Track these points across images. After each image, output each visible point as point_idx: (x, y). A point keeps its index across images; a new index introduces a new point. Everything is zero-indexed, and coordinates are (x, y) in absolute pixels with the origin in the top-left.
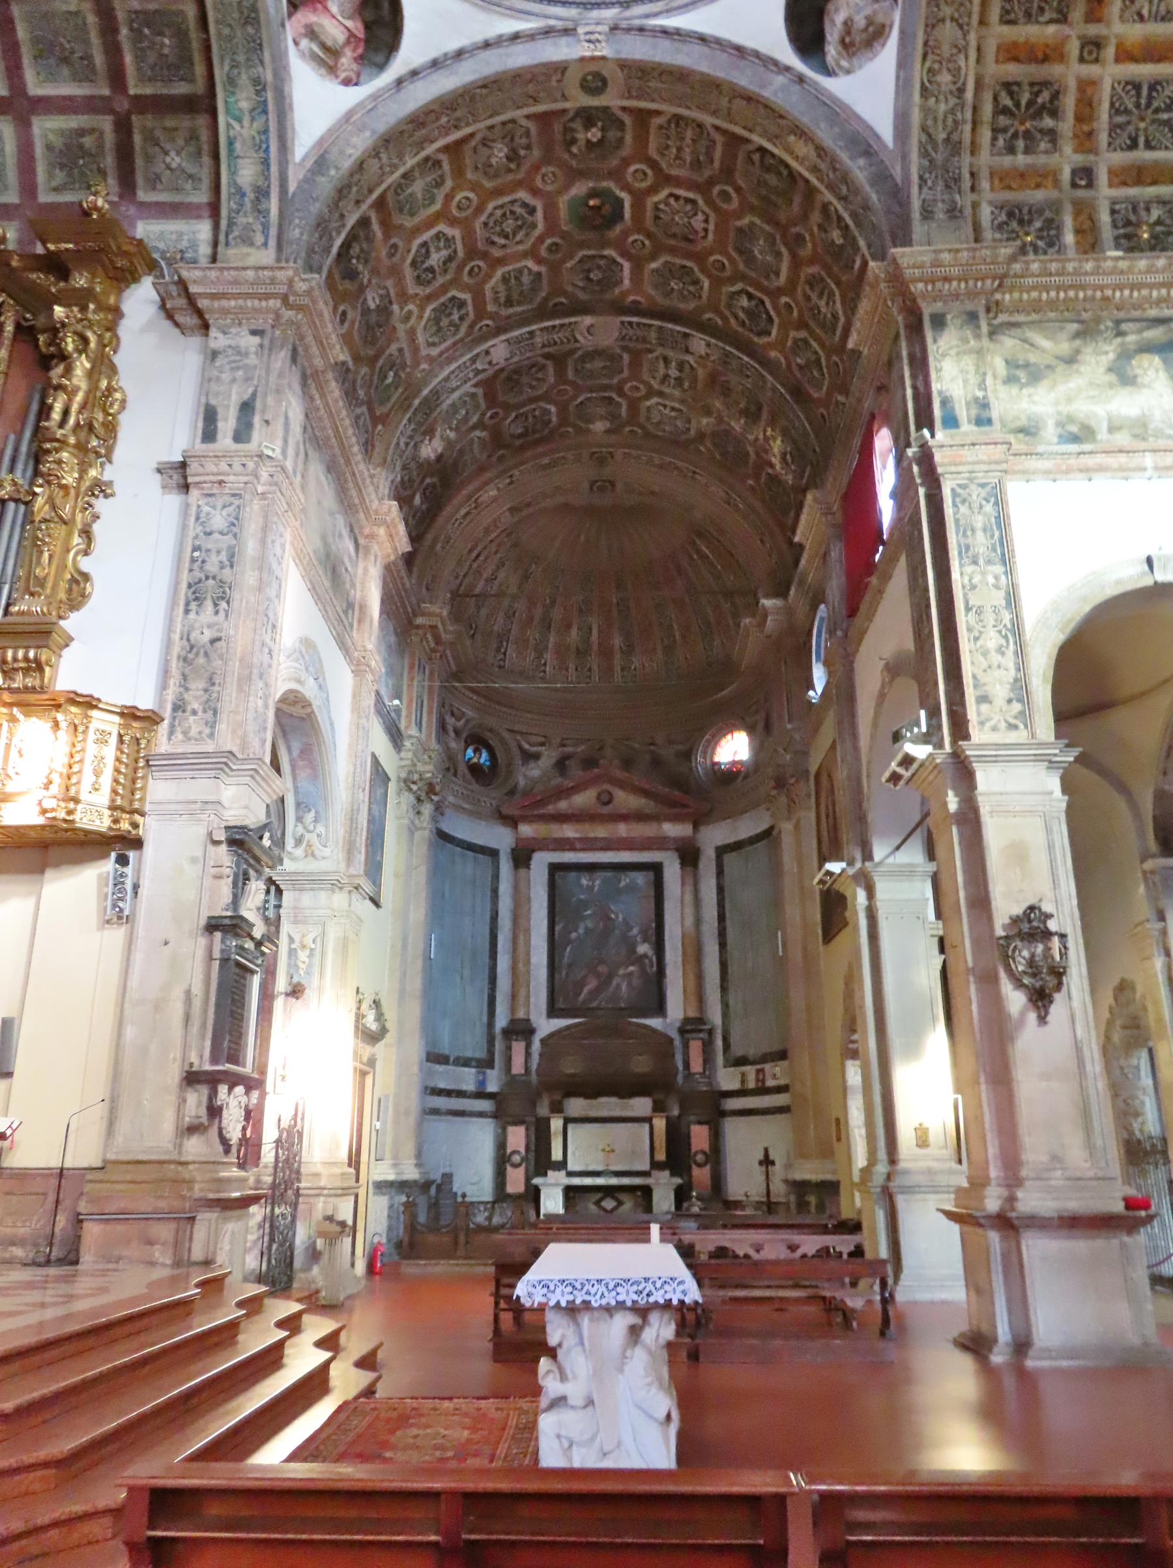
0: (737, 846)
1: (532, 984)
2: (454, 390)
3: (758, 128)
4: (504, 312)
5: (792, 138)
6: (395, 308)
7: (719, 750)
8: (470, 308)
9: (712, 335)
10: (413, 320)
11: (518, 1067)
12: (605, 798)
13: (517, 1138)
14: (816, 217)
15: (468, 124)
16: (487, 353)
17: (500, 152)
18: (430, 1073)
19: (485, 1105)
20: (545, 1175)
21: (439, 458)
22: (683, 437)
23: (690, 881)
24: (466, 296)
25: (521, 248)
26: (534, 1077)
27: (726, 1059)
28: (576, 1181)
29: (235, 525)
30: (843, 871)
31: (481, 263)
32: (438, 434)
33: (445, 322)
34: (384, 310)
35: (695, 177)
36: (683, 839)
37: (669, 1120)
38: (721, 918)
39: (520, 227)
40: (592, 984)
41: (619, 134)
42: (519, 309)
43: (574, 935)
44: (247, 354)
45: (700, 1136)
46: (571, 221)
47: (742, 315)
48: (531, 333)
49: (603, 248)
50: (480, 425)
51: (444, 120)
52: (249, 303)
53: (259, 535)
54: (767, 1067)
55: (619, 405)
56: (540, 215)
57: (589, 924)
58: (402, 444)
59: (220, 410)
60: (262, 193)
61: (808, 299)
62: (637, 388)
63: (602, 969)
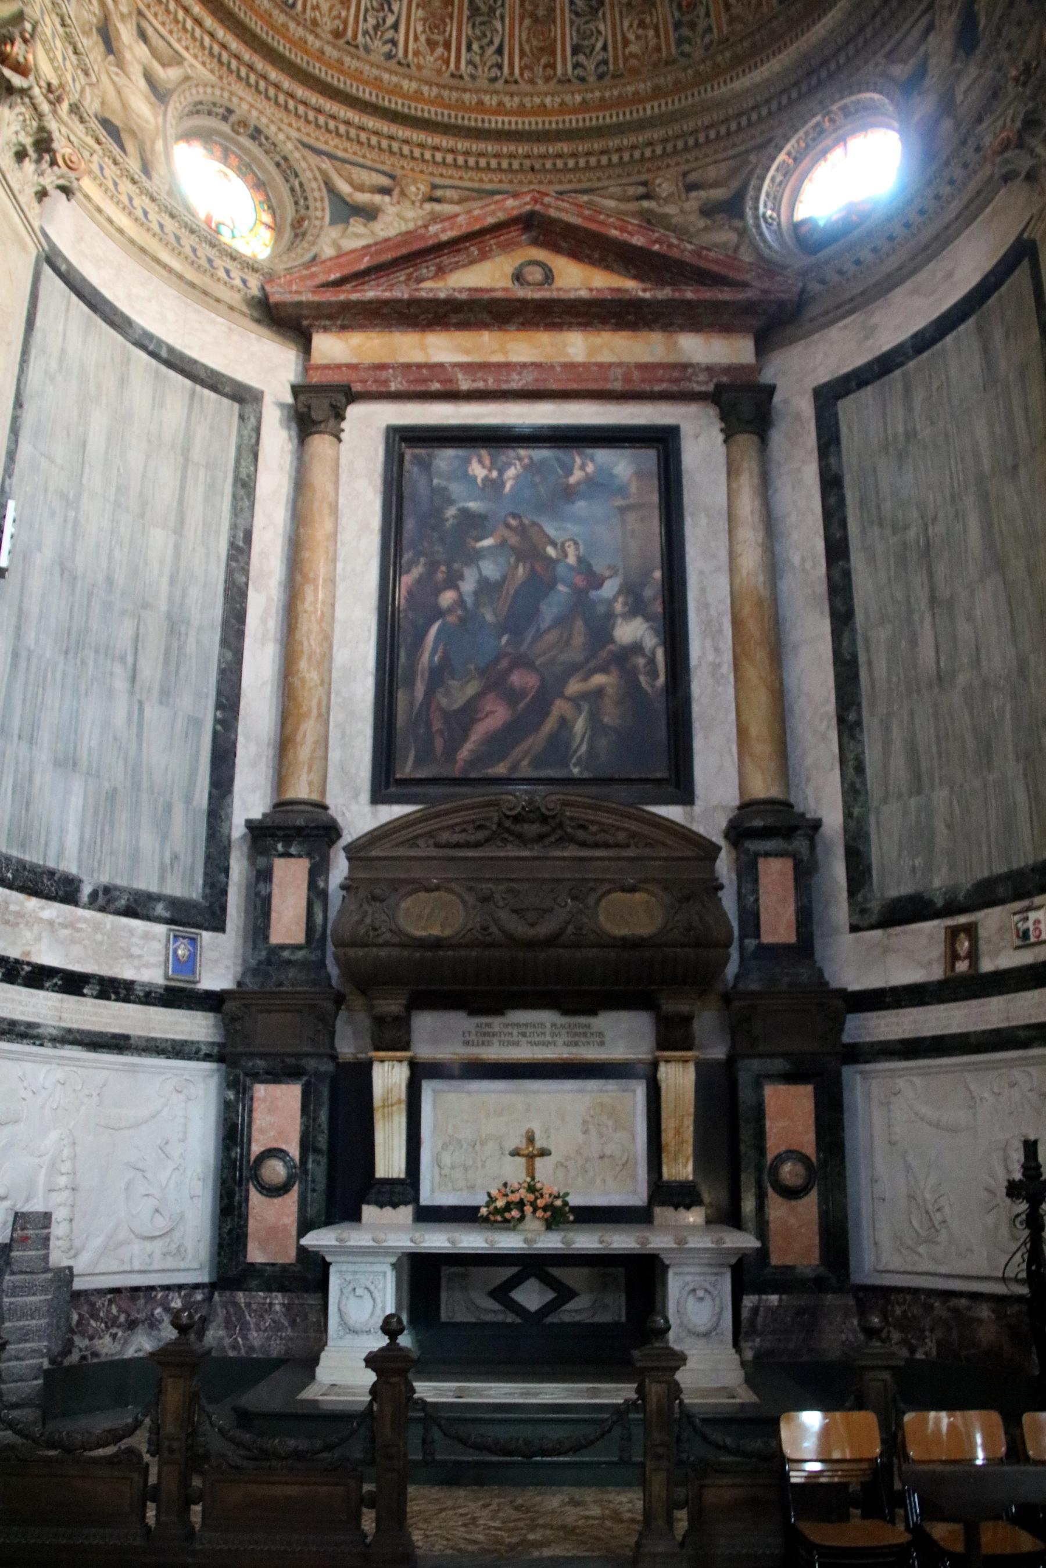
1: (336, 717)
13: (279, 1114)
19: (195, 1026)
20: (355, 1217)
28: (437, 1240)
36: (728, 369)
37: (703, 1070)
38: (837, 550)
40: (496, 715)
43: (447, 598)
45: (788, 1115)
54: (991, 921)
57: (490, 569)
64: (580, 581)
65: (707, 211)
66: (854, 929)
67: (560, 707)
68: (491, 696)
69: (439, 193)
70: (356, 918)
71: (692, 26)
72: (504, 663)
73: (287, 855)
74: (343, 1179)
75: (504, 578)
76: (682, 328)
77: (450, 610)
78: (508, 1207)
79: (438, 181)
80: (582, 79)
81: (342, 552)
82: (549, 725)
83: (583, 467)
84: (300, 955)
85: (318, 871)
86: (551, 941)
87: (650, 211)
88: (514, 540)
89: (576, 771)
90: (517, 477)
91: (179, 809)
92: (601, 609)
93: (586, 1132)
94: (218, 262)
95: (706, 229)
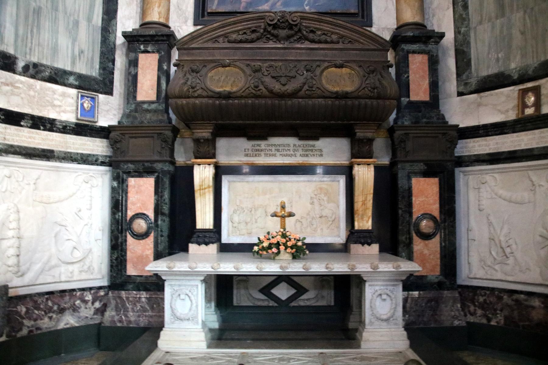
13: (142, 194)
19: (97, 146)
20: (185, 250)
28: (229, 266)
37: (378, 169)
45: (425, 194)
66: (460, 94)
70: (182, 81)
74: (178, 231)
78: (270, 247)
84: (153, 106)
86: (294, 95)
89: (307, 8)
91: (83, 24)
93: (312, 203)
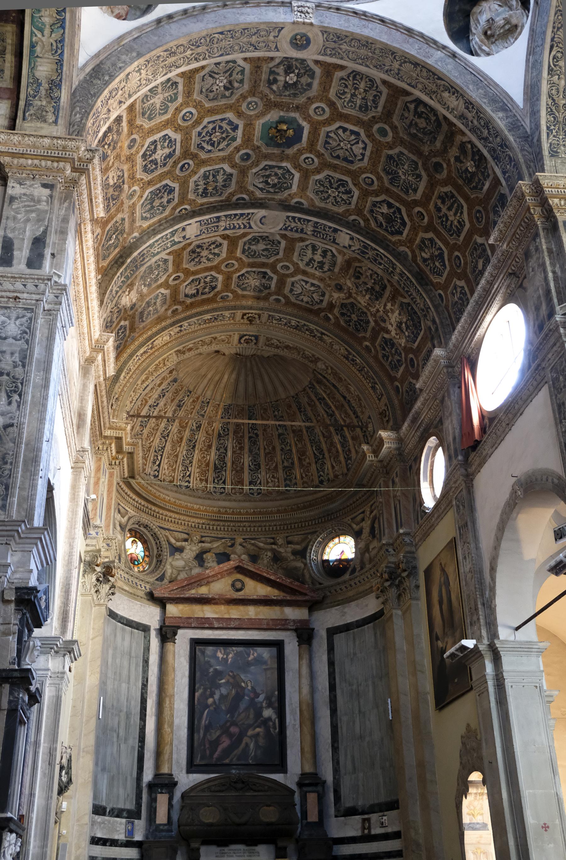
0: (347, 628)
1: (175, 742)
2: (155, 255)
3: (420, 86)
4: (200, 201)
5: (446, 94)
6: (126, 186)
7: (327, 550)
8: (176, 195)
9: (358, 232)
10: (135, 198)
11: (161, 817)
12: (239, 585)
14: (454, 152)
15: (204, 59)
16: (184, 229)
17: (222, 81)
18: (93, 823)
21: (133, 306)
22: (316, 307)
23: (306, 657)
24: (176, 185)
25: (221, 154)
26: (175, 826)
27: (337, 810)
29: (27, 334)
30: (476, 646)
31: (191, 162)
32: (135, 288)
33: (157, 203)
34: (118, 187)
35: (361, 115)
36: (300, 621)
38: (332, 688)
39: (224, 139)
40: (226, 742)
41: (309, 80)
42: (212, 200)
43: (210, 701)
44: (39, 201)
46: (262, 138)
47: (380, 218)
48: (218, 218)
49: (281, 161)
50: (166, 285)
51: (189, 52)
52: (43, 163)
53: (44, 344)
54: (374, 817)
55: (271, 278)
56: (240, 132)
57: (224, 691)
58: (114, 292)
59: (16, 242)
60: (55, 85)
61: (439, 210)
62: (287, 268)
63: (234, 730)
64: (252, 695)
65: (294, 553)
66: (336, 816)
67: (246, 740)
68: (224, 736)
69: (203, 539)
70: (187, 816)
71: (291, 481)
72: (228, 724)
73: (161, 793)
75: (228, 694)
76: (285, 606)
77: (211, 705)
79: (203, 534)
80: (253, 494)
81: (176, 684)
82: (243, 745)
83: (253, 654)
84: (166, 827)
85: (171, 799)
86: (245, 824)
87: (275, 549)
88: (231, 680)
90: (232, 658)
91: (129, 778)
92: (259, 705)
94: (138, 583)
95: (293, 560)
